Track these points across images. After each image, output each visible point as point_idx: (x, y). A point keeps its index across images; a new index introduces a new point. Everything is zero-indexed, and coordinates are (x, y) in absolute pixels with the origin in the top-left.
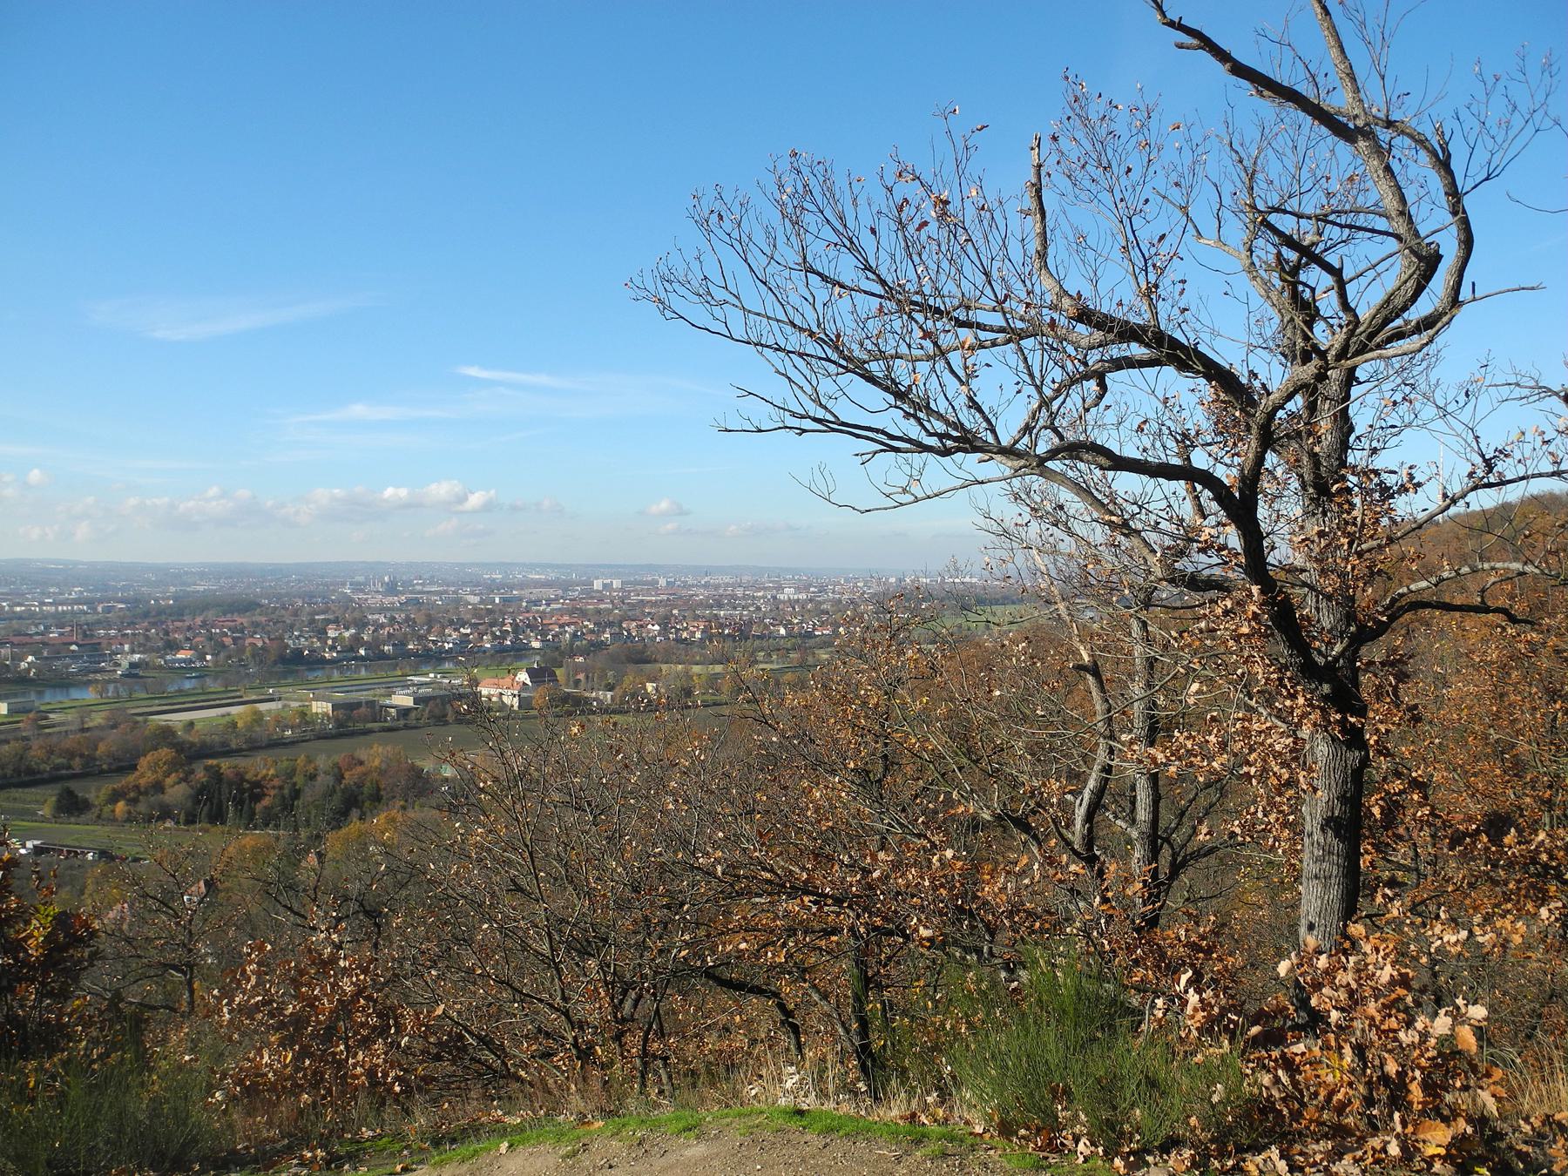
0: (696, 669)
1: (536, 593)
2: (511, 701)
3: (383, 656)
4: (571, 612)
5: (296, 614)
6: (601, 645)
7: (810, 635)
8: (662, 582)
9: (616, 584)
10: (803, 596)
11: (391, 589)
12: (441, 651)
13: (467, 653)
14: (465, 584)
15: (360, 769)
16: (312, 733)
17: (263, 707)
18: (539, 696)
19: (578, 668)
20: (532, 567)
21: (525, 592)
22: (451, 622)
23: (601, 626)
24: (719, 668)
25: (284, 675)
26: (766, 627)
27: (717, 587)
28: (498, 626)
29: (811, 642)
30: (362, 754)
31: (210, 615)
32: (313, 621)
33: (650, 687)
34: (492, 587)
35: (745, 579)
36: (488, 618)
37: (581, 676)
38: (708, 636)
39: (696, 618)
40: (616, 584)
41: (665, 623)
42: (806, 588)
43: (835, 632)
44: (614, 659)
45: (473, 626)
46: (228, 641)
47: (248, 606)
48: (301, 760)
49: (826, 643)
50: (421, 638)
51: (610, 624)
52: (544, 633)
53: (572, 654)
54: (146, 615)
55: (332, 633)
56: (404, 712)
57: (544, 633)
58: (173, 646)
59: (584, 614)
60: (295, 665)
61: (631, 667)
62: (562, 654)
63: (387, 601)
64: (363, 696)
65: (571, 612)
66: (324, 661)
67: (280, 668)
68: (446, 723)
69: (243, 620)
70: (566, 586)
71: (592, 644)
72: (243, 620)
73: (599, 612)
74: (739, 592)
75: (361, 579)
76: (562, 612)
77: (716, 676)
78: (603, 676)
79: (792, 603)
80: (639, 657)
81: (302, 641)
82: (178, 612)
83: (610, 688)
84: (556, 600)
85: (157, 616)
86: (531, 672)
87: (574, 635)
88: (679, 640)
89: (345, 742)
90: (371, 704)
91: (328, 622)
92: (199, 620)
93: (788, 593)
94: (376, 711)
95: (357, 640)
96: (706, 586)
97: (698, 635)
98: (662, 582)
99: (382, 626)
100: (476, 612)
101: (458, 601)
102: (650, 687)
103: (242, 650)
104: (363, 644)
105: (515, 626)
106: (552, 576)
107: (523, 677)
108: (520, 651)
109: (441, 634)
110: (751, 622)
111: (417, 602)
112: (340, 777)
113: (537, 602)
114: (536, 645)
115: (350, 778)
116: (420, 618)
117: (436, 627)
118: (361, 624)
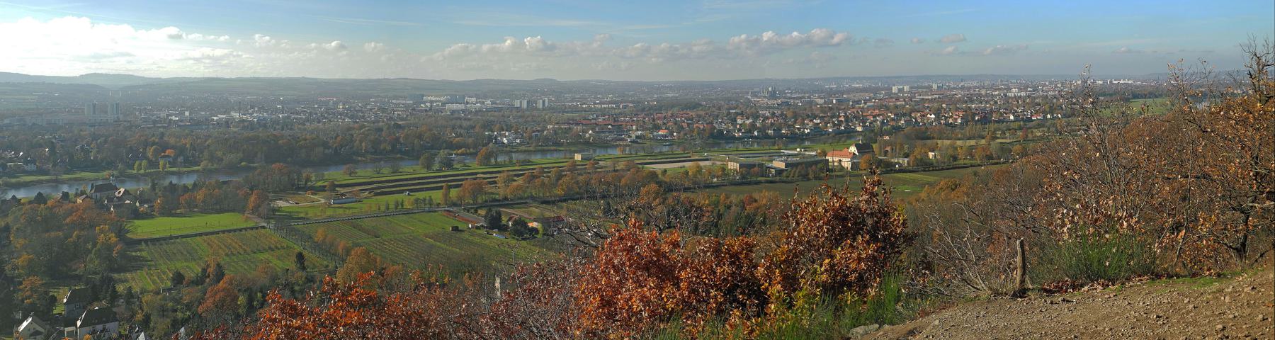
0: (959, 143)
1: (858, 96)
2: (847, 164)
3: (768, 137)
4: (880, 108)
5: (719, 109)
6: (898, 129)
7: (1030, 120)
8: (935, 86)
9: (906, 88)
10: (1023, 94)
11: (773, 95)
13: (817, 135)
14: (815, 92)
15: (755, 205)
19: (886, 143)
20: (854, 79)
24: (973, 142)
27: (969, 89)
29: (1031, 124)
30: (756, 196)
31: (675, 110)
32: (729, 114)
33: (931, 155)
34: (831, 93)
35: (987, 83)
36: (829, 113)
37: (888, 149)
38: (966, 121)
39: (957, 109)
40: (906, 88)
41: (938, 113)
43: (1045, 117)
44: (908, 137)
45: (821, 118)
46: (685, 125)
47: (695, 106)
48: (722, 197)
49: (1040, 125)
50: (789, 126)
51: (905, 115)
52: (864, 122)
53: (882, 134)
54: (643, 110)
55: (739, 121)
58: (657, 128)
59: (887, 108)
61: (919, 142)
62: (876, 134)
64: (757, 160)
65: (880, 108)
68: (809, 179)
69: (693, 114)
70: (876, 91)
71: (893, 128)
72: (693, 114)
73: (897, 107)
74: (983, 92)
76: (874, 108)
77: (971, 147)
79: (1017, 98)
80: (923, 135)
81: (725, 127)
82: (659, 109)
83: (906, 156)
84: (870, 100)
86: (858, 146)
87: (882, 122)
88: (947, 124)
89: (746, 188)
90: (761, 165)
91: (737, 114)
94: (764, 170)
95: (753, 126)
96: (962, 88)
98: (935, 86)
99: (768, 118)
100: (823, 109)
101: (811, 103)
102: (931, 155)
104: (757, 128)
106: (867, 85)
107: (853, 149)
108: (850, 133)
109: (803, 124)
110: (992, 112)
111: (787, 103)
112: (744, 208)
113: (858, 102)
114: (859, 129)
115: (749, 209)
116: (789, 114)
117: (800, 120)
118: (756, 117)
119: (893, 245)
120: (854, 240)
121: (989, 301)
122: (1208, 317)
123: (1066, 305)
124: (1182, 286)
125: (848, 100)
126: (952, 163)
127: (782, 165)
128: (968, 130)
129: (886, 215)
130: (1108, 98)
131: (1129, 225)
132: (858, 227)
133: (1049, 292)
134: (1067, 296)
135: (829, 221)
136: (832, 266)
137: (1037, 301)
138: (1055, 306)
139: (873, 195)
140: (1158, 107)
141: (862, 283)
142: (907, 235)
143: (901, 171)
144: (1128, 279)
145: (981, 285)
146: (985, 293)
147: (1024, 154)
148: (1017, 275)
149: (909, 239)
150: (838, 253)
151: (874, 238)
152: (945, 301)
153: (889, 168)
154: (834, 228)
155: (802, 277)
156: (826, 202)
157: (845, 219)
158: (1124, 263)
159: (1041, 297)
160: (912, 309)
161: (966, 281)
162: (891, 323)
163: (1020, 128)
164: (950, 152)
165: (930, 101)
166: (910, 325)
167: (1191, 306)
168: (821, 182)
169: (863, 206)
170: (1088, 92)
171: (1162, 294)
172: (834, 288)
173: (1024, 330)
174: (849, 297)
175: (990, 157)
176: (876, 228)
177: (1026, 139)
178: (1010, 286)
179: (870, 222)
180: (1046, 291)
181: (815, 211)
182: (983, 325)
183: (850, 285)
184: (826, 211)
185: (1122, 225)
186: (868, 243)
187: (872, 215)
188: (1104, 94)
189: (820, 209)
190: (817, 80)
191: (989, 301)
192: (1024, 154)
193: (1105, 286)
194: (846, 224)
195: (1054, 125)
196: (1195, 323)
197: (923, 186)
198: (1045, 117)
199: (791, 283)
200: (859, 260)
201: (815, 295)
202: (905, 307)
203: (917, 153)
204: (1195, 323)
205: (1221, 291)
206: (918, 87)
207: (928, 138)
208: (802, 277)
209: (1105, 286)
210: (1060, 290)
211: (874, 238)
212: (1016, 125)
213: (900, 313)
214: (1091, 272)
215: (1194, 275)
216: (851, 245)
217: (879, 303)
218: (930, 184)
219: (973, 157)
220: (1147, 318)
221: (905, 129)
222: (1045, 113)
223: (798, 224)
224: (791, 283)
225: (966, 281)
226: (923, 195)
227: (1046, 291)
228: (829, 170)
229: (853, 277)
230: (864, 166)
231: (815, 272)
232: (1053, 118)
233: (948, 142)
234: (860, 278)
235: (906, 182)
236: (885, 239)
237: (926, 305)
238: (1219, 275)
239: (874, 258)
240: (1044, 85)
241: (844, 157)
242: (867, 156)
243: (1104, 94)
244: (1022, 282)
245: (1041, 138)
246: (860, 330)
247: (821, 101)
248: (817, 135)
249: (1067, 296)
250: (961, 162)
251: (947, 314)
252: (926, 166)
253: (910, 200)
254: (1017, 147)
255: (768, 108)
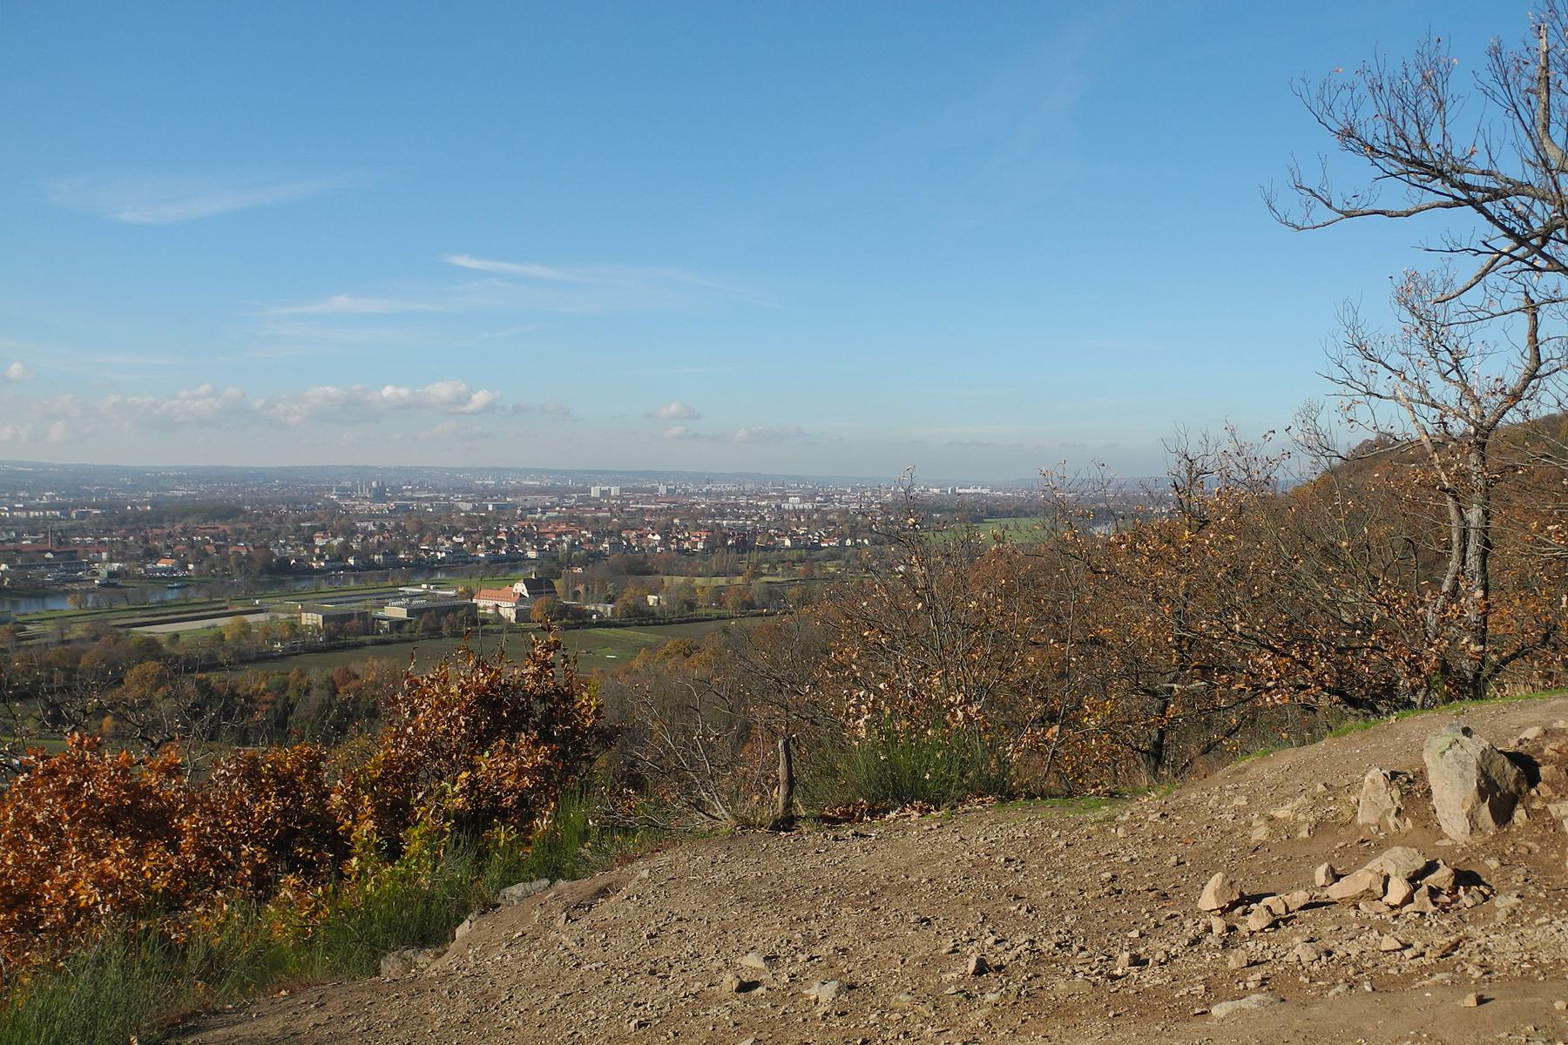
0: (699, 581)
2: (508, 612)
3: (373, 566)
4: (568, 521)
6: (598, 556)
7: (817, 547)
8: (662, 489)
9: (615, 491)
10: (808, 506)
11: (379, 495)
12: (434, 560)
13: (459, 562)
14: (456, 490)
15: (354, 683)
16: (302, 647)
17: (250, 619)
18: (537, 608)
19: (577, 579)
20: (526, 472)
21: (520, 499)
22: (443, 531)
23: (600, 535)
24: (722, 581)
25: (270, 585)
26: (771, 537)
27: (719, 495)
28: (491, 534)
30: (356, 668)
33: (652, 599)
34: (485, 493)
35: (748, 487)
36: (480, 526)
37: (581, 588)
38: (711, 547)
39: (698, 527)
40: (615, 491)
42: (812, 498)
43: (842, 543)
45: (466, 534)
46: (211, 549)
47: (230, 512)
49: (833, 556)
50: (412, 547)
51: (610, 534)
52: (540, 543)
53: (570, 564)
54: (123, 521)
55: (319, 542)
56: (398, 625)
57: (540, 543)
59: (581, 523)
60: (281, 575)
61: (632, 578)
62: (560, 565)
63: (376, 507)
64: (355, 608)
65: (568, 521)
66: (311, 571)
67: (266, 578)
68: (441, 637)
70: (563, 493)
73: (597, 520)
74: (742, 501)
75: (347, 484)
76: (558, 520)
77: (719, 589)
78: (603, 588)
79: (797, 513)
80: (640, 567)
81: (291, 551)
83: (611, 600)
84: (552, 508)
85: (135, 521)
86: (528, 583)
87: (572, 545)
89: (339, 655)
90: (363, 616)
91: (315, 529)
92: (179, 527)
93: (794, 502)
94: (369, 624)
95: (346, 550)
96: (708, 494)
97: (700, 546)
98: (662, 489)
99: (372, 534)
100: (469, 520)
101: (450, 509)
102: (652, 599)
103: (226, 559)
104: (351, 552)
105: (510, 534)
106: (547, 482)
107: (520, 588)
108: (515, 562)
109: (434, 543)
110: (755, 533)
111: (406, 508)
113: (532, 510)
114: (532, 554)
116: (410, 525)
118: (350, 532)
119: (579, 747)
120: (513, 739)
121: (733, 837)
122: (1087, 859)
123: (858, 843)
124: (1051, 812)
125: (515, 507)
126: (686, 613)
127: (402, 614)
128: (714, 561)
129: (568, 698)
130: (947, 517)
131: (966, 716)
132: (519, 720)
133: (833, 821)
134: (862, 828)
135: (469, 708)
136: (473, 783)
137: (812, 836)
138: (842, 844)
139: (546, 665)
140: (1025, 533)
141: (525, 810)
142: (602, 731)
143: (602, 624)
144: (962, 801)
145: (720, 811)
146: (727, 823)
147: (803, 601)
148: (779, 794)
149: (606, 737)
150: (484, 761)
151: (546, 737)
152: (661, 837)
153: (580, 619)
154: (476, 721)
155: (420, 803)
156: (462, 675)
157: (498, 705)
158: (955, 775)
159: (819, 830)
160: (606, 852)
161: (699, 805)
162: (574, 878)
163: (801, 560)
164: (684, 595)
165: (654, 513)
166: (600, 879)
167: (1062, 843)
168: (460, 642)
169: (530, 684)
170: (910, 505)
171: (1016, 824)
172: (474, 822)
173: (789, 882)
174: (502, 834)
175: (749, 605)
176: (549, 718)
177: (809, 578)
178: (768, 812)
179: (540, 708)
180: (827, 819)
181: (446, 692)
182: (721, 876)
183: (504, 815)
184: (465, 692)
185: (954, 715)
186: (536, 744)
187: (543, 698)
188: (940, 510)
189: (454, 689)
190: (463, 470)
191: (733, 837)
192: (803, 601)
193: (924, 812)
194: (497, 714)
195: (856, 556)
196: (1067, 870)
197: (637, 649)
198: (842, 543)
199: (395, 816)
200: (521, 772)
201: (443, 833)
202: (597, 849)
203: (629, 596)
204: (1067, 870)
205: (1112, 819)
206: (635, 490)
207: (649, 574)
208: (420, 803)
209: (924, 812)
210: (849, 818)
211: (546, 737)
212: (795, 554)
213: (586, 860)
214: (898, 789)
215: (1070, 794)
216: (507, 749)
217: (553, 844)
218: (649, 647)
219: (721, 604)
220: (990, 862)
221: (602, 559)
222: (843, 537)
223: (414, 713)
224: (395, 816)
225: (699, 805)
226: (637, 664)
227: (827, 819)
228: (475, 622)
229: (509, 801)
230: (537, 615)
231: (443, 792)
232: (855, 545)
233: (681, 579)
234: (522, 802)
235: (608, 643)
236: (565, 738)
237: (630, 846)
238: (1112, 795)
239: (544, 770)
240: (845, 493)
241: (502, 601)
242: (544, 600)
243: (940, 510)
244: (789, 805)
245: (833, 576)
246: (516, 890)
247: (469, 506)
248: (459, 562)
249: (862, 828)
250: (702, 611)
251: (663, 859)
252: (641, 617)
253: (613, 673)
254: (794, 591)
255: (371, 517)
